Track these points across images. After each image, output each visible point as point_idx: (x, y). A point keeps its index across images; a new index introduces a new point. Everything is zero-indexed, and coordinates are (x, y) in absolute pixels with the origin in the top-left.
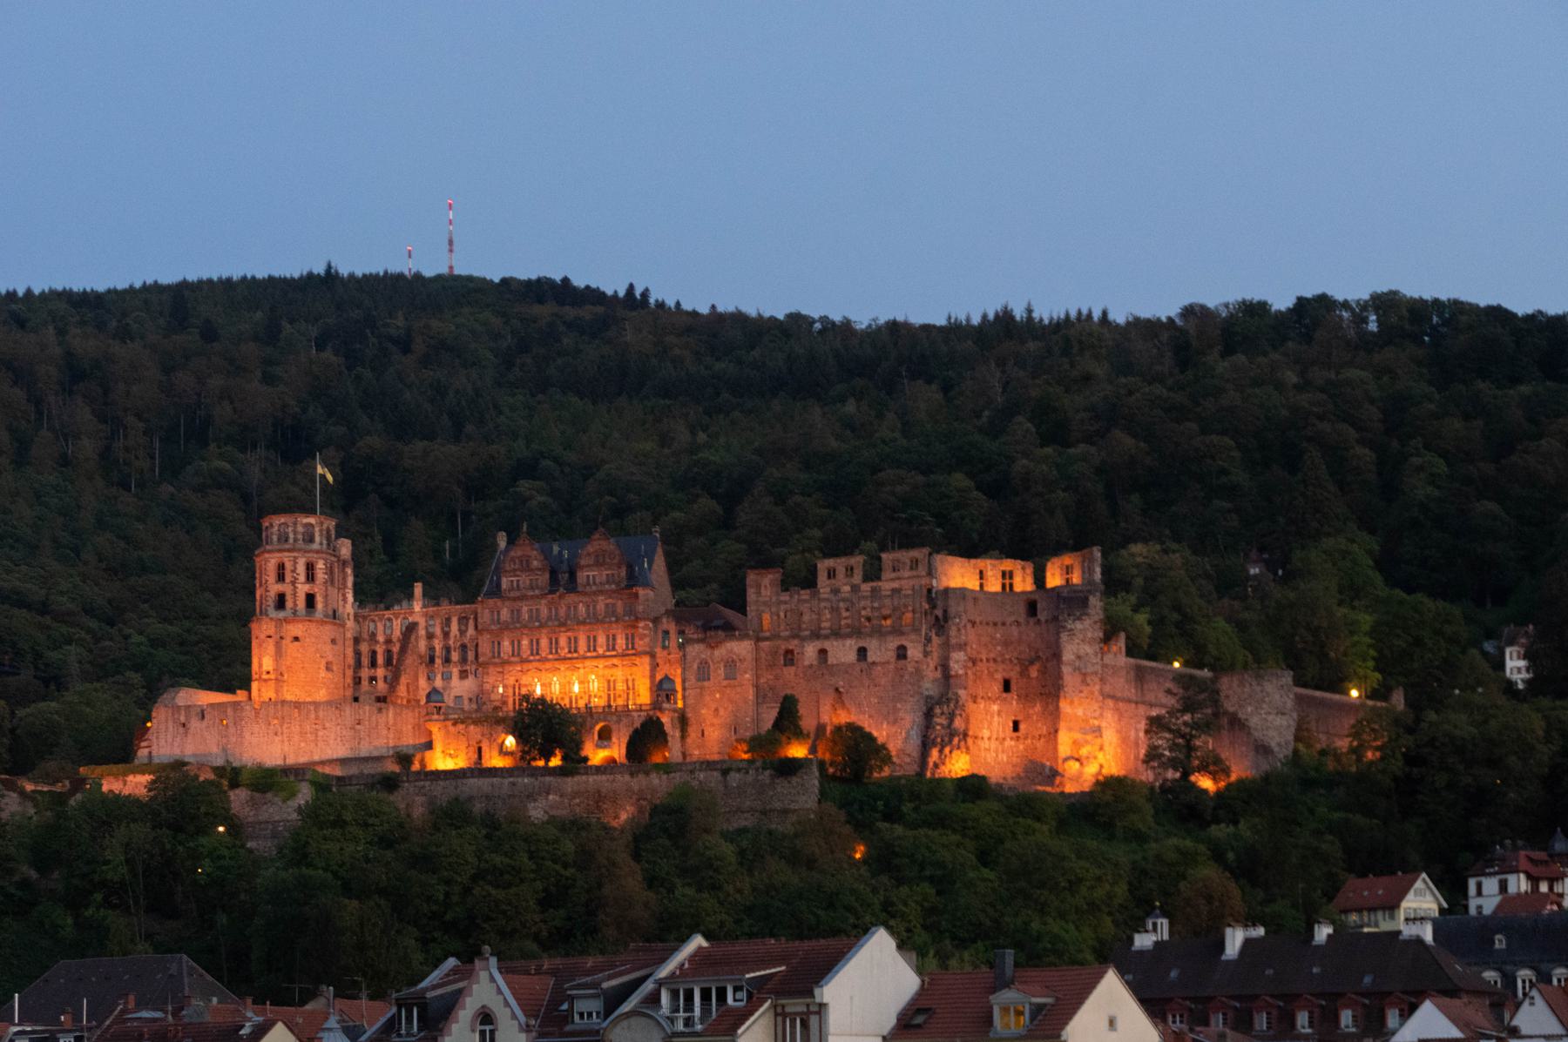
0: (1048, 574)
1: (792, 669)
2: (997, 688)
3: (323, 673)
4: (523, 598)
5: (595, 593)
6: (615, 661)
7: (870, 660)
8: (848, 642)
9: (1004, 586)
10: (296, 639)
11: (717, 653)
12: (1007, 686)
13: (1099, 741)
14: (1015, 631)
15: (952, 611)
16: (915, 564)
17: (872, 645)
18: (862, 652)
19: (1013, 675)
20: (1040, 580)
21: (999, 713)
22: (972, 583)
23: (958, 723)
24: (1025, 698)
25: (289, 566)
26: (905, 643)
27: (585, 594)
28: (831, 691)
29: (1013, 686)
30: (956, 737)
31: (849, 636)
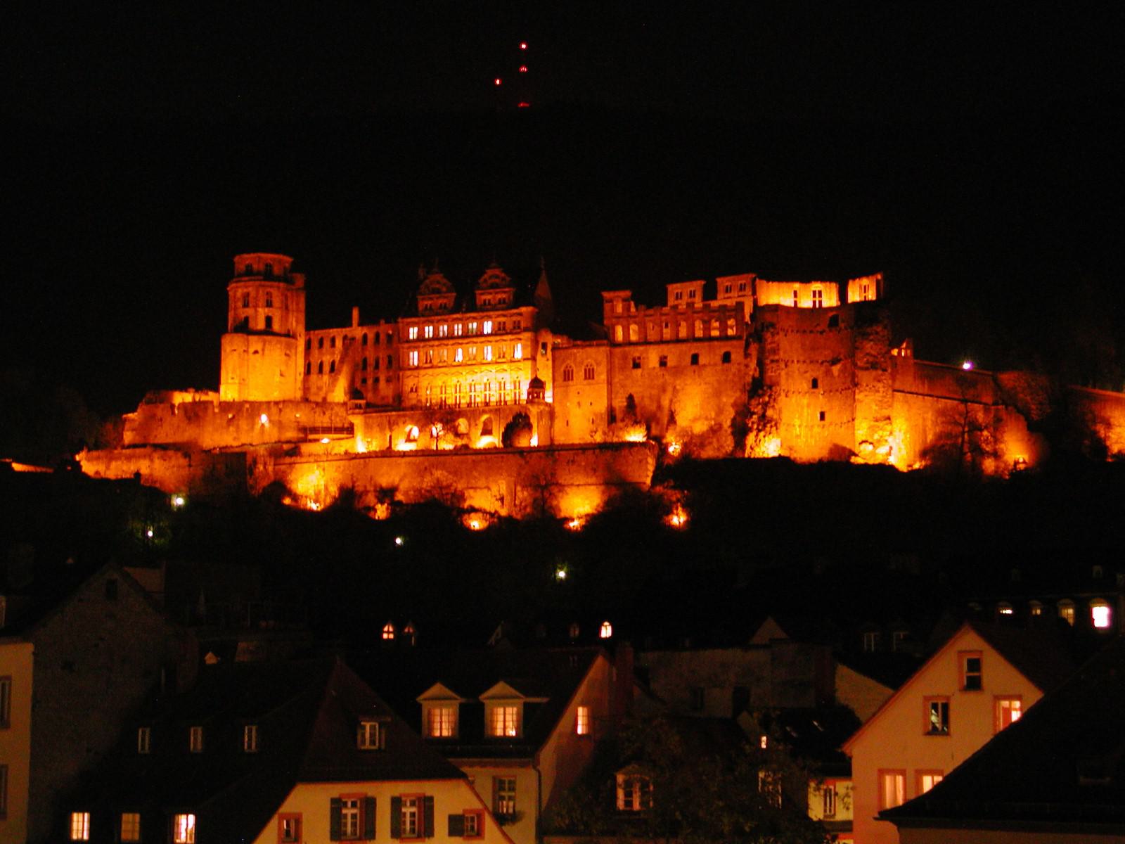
0: (850, 294)
1: (639, 371)
2: (806, 386)
3: (277, 378)
6: (505, 366)
9: (814, 302)
10: (256, 352)
12: (815, 384)
13: (889, 428)
16: (742, 288)
18: (695, 359)
19: (819, 373)
20: (843, 295)
21: (808, 406)
22: (788, 301)
24: (829, 391)
25: (253, 294)
30: (766, 423)
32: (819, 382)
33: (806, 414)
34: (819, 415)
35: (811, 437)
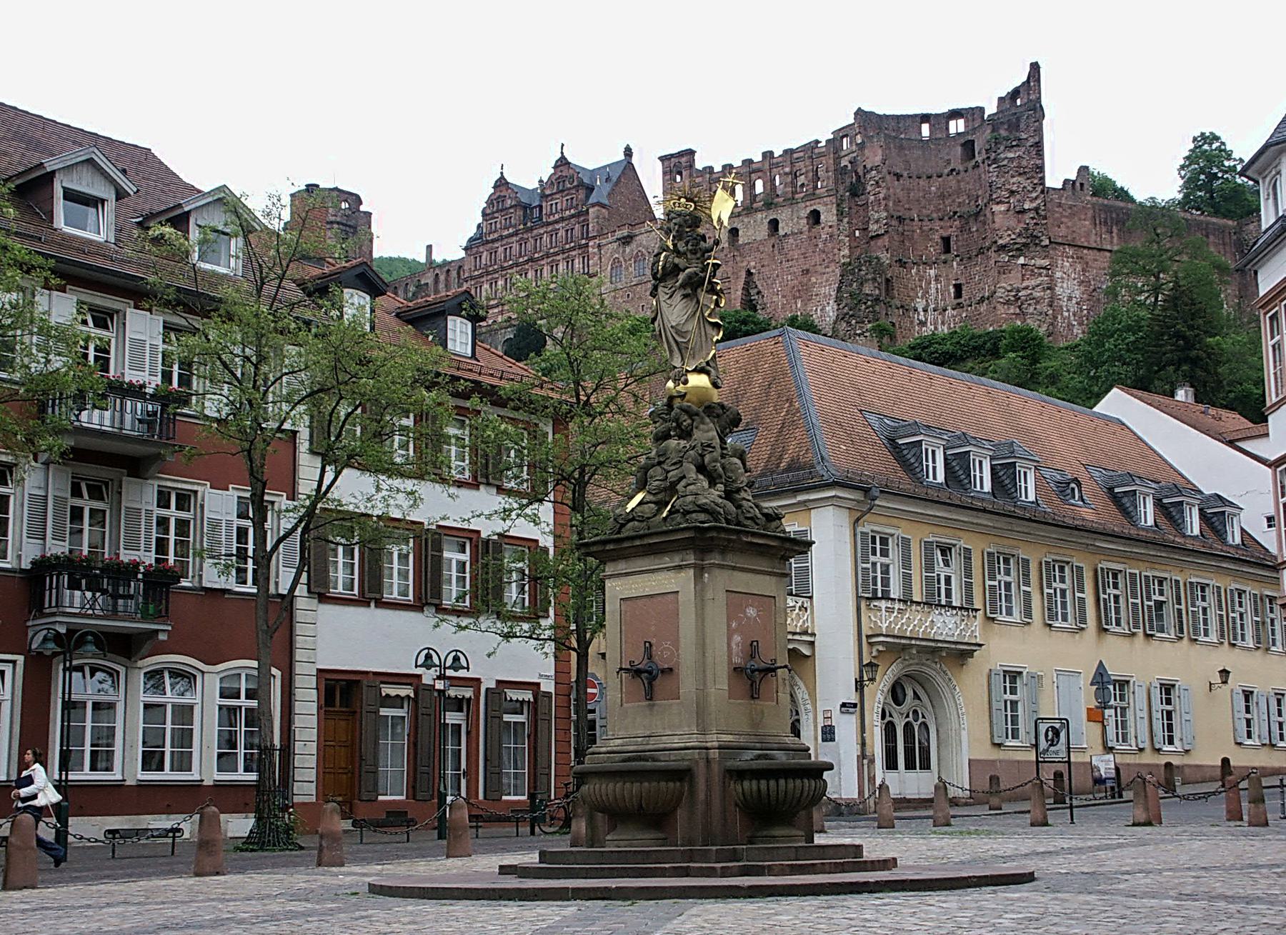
2: (933, 250)
4: (502, 238)
5: (556, 222)
7: (781, 232)
8: (759, 215)
11: (628, 250)
14: (952, 181)
15: (869, 166)
17: (783, 215)
18: (774, 224)
21: (937, 279)
23: (867, 289)
24: (966, 259)
26: (820, 208)
27: (549, 224)
28: (743, 274)
29: (953, 246)
31: (757, 210)
32: (953, 239)
33: (933, 291)
34: (952, 290)
35: (943, 323)
